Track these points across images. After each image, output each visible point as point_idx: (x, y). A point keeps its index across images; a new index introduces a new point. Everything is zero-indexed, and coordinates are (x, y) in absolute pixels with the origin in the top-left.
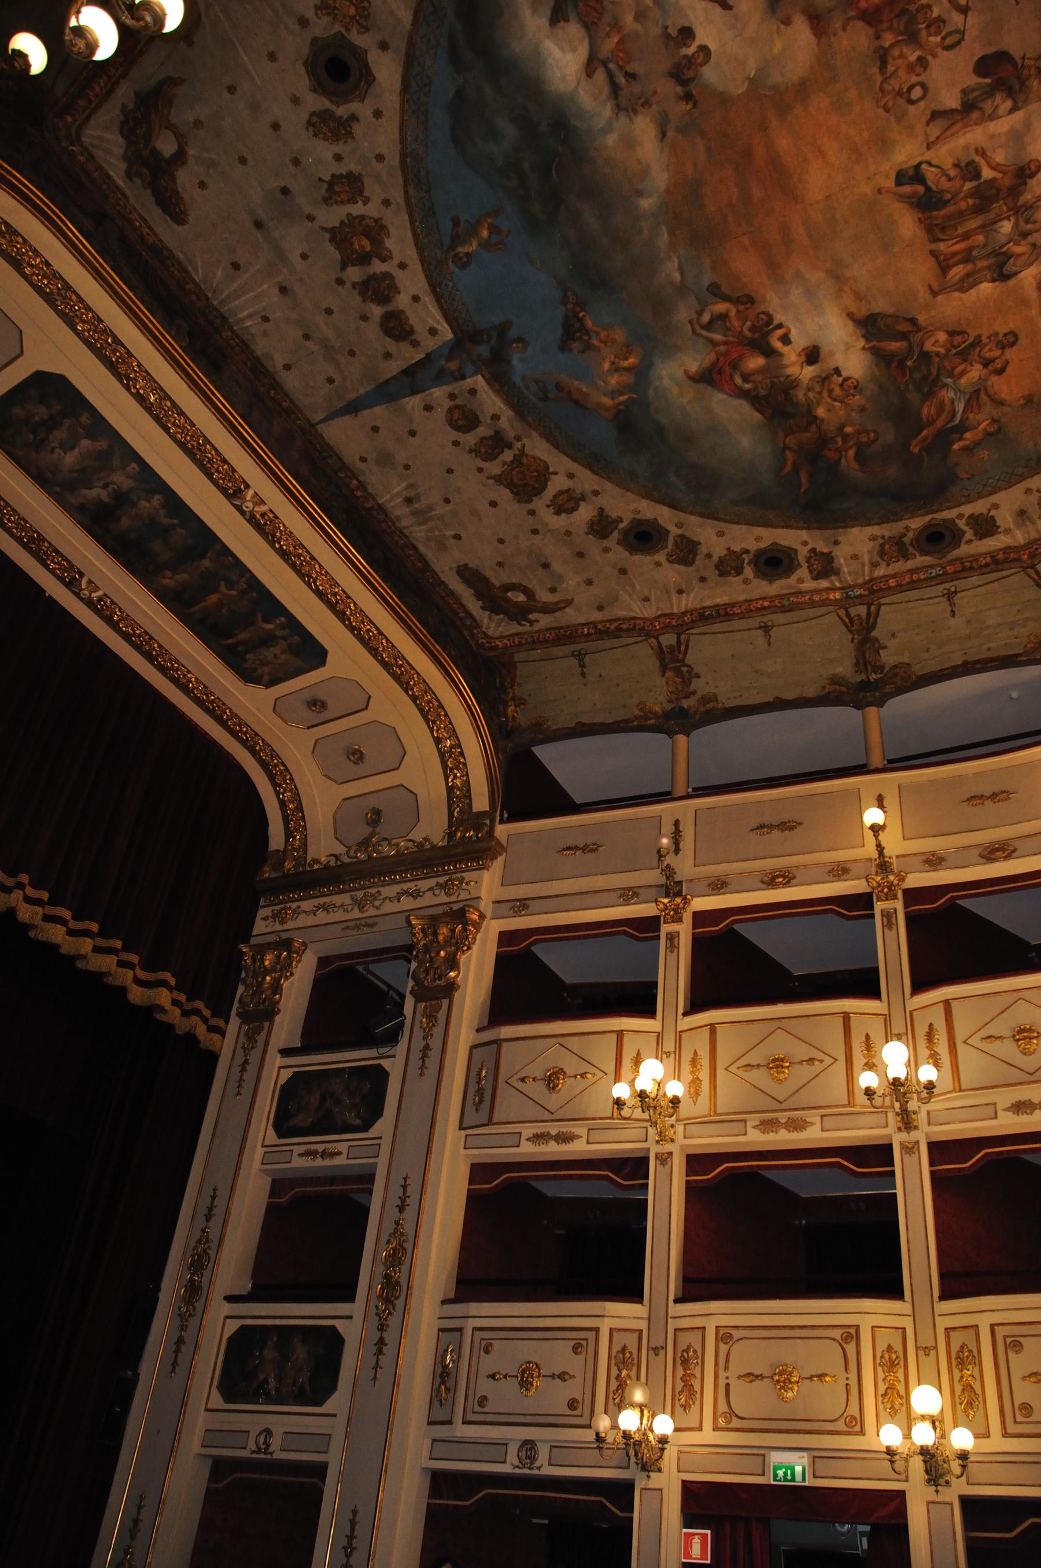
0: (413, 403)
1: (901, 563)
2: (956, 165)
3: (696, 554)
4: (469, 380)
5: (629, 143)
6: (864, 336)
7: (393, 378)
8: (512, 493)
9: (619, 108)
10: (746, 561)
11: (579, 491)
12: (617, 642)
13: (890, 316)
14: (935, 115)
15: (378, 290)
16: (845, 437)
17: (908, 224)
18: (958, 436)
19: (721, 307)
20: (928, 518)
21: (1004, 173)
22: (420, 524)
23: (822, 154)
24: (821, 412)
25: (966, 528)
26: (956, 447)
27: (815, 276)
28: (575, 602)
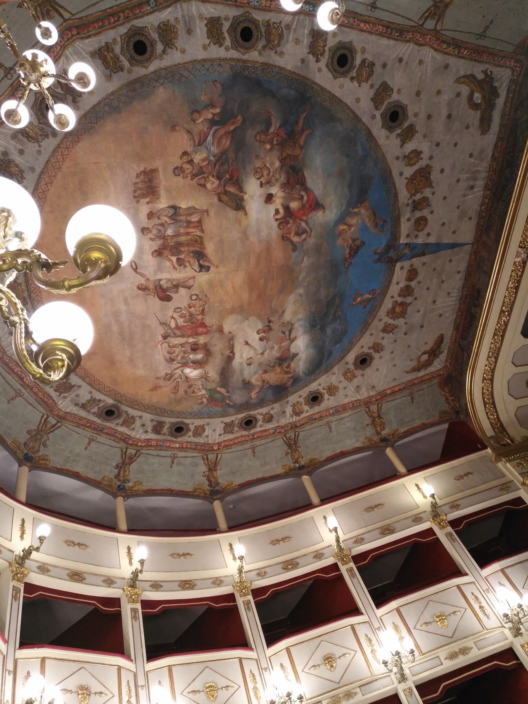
0: (432, 240)
1: (273, 20)
2: (185, 266)
3: (378, 89)
4: (405, 242)
5: (295, 313)
6: (243, 200)
7: (430, 254)
8: (430, 174)
9: (292, 325)
10: (356, 69)
11: (404, 163)
12: (457, 36)
13: (229, 206)
14: (189, 288)
15: (407, 291)
16: (271, 142)
17: (210, 248)
18: (216, 118)
19: (296, 239)
20: (246, 57)
21: (167, 257)
22: (478, 171)
23: (233, 287)
24: (277, 164)
25: (226, 35)
26: (218, 110)
27: (253, 239)
28: (455, 78)
